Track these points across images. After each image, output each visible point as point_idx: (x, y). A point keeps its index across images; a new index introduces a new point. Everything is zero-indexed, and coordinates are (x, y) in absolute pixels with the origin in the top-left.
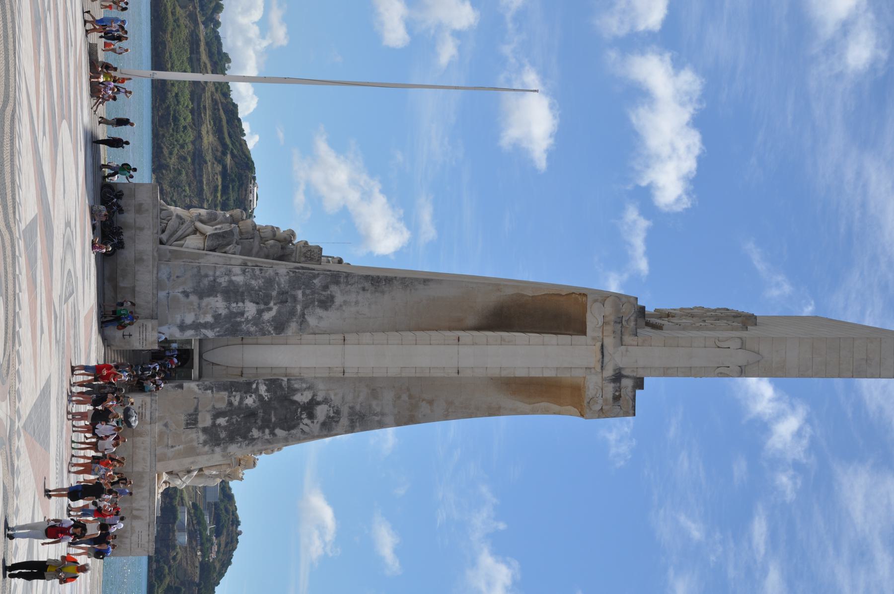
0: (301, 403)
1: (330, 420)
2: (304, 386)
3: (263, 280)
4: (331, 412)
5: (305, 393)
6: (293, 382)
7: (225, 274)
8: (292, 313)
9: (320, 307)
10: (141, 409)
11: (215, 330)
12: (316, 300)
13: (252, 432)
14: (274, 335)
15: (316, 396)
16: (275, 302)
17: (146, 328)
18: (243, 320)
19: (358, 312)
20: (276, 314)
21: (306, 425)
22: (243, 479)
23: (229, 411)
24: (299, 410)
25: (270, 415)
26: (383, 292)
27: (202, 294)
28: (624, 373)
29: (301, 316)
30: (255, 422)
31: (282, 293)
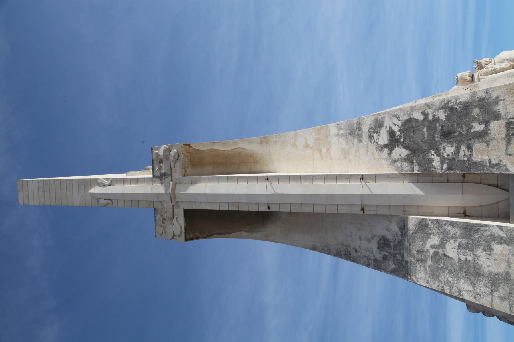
0: (401, 146)
1: (376, 130)
2: (399, 164)
3: (440, 279)
4: (376, 138)
6: (409, 168)
7: (480, 295)
9: (388, 240)
11: (489, 233)
13: (445, 116)
15: (388, 154)
16: (428, 254)
18: (459, 240)
21: (395, 125)
23: (470, 139)
24: (402, 140)
26: (343, 244)
30: (443, 127)
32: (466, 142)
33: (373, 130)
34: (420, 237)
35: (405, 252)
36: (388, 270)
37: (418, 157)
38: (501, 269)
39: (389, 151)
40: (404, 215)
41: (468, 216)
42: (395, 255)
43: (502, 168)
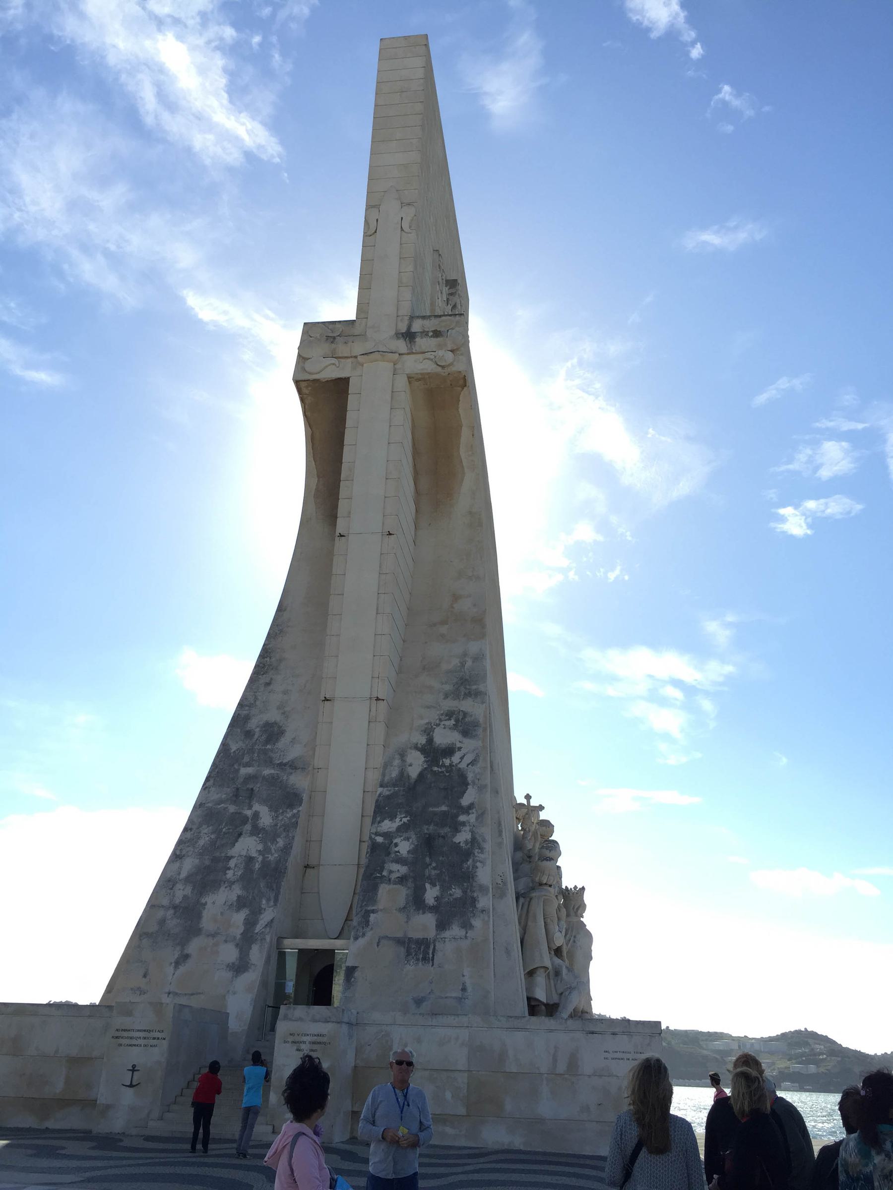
0: (425, 766)
2: (397, 762)
4: (447, 723)
5: (409, 759)
6: (387, 779)
7: (171, 889)
8: (273, 781)
9: (277, 740)
11: (263, 906)
13: (460, 843)
14: (300, 809)
15: (417, 744)
18: (260, 858)
21: (462, 758)
24: (436, 769)
25: (435, 814)
26: (280, 661)
27: (192, 930)
28: (403, 328)
29: (282, 769)
30: (443, 837)
35: (253, 768)
36: (228, 739)
38: (207, 922)
39: (420, 746)
41: (305, 871)
42: (251, 751)
43: (361, 930)
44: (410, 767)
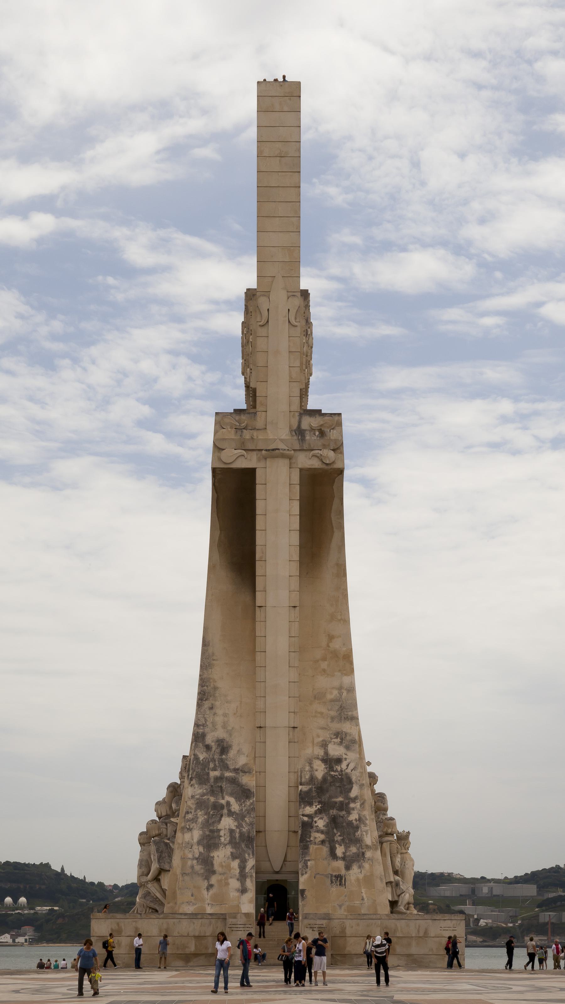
1: (344, 742)
2: (307, 768)
3: (198, 811)
4: (335, 740)
5: (315, 767)
6: (303, 780)
7: (191, 848)
8: (233, 781)
10: (315, 929)
11: (247, 858)
12: (220, 757)
13: (352, 820)
15: (318, 756)
16: (221, 799)
17: (234, 925)
18: (238, 830)
19: (235, 714)
20: (233, 797)
21: (348, 766)
22: (409, 831)
23: (330, 844)
24: (332, 773)
25: (336, 803)
26: (215, 688)
30: (342, 817)
31: (212, 792)
32: (327, 839)
33: (344, 737)
34: (236, 790)
37: (315, 791)
40: (256, 772)
42: (213, 760)
43: (304, 870)
44: (316, 772)
